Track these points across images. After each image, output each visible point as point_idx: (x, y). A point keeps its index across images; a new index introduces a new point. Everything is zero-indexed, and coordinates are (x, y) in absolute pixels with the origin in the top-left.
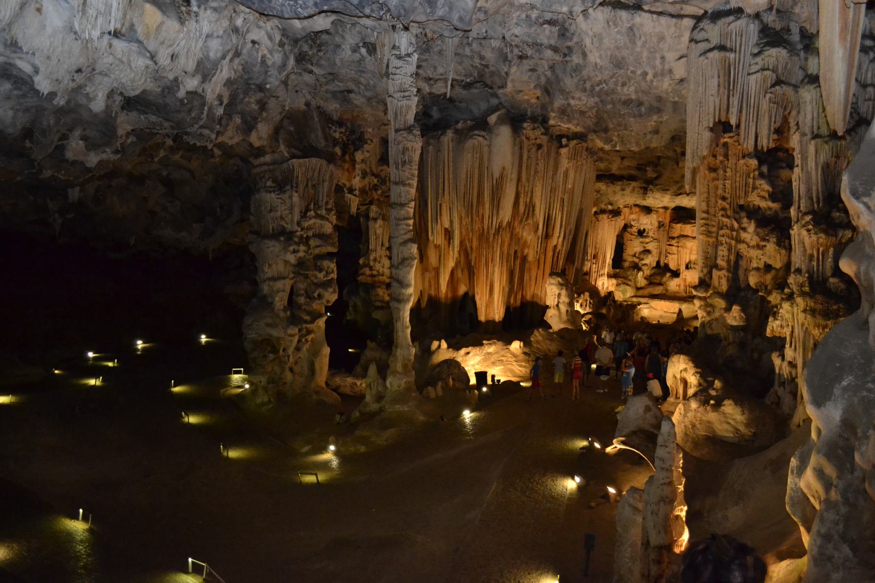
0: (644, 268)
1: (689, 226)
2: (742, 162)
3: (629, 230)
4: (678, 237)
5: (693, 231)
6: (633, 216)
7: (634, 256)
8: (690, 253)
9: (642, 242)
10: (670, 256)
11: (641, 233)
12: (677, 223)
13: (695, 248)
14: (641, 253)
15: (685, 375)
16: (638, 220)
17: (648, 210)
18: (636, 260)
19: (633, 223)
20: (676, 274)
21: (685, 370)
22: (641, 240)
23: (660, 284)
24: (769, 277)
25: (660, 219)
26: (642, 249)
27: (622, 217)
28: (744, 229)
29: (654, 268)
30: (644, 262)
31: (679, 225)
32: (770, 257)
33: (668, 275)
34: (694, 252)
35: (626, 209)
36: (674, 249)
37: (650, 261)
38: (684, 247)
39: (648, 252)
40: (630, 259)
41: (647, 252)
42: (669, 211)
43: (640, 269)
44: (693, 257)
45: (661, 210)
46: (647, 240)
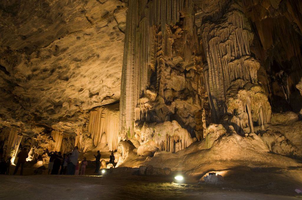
2: (170, 39)
15: (177, 133)
21: (177, 130)
24: (177, 94)
28: (165, 70)
32: (175, 86)
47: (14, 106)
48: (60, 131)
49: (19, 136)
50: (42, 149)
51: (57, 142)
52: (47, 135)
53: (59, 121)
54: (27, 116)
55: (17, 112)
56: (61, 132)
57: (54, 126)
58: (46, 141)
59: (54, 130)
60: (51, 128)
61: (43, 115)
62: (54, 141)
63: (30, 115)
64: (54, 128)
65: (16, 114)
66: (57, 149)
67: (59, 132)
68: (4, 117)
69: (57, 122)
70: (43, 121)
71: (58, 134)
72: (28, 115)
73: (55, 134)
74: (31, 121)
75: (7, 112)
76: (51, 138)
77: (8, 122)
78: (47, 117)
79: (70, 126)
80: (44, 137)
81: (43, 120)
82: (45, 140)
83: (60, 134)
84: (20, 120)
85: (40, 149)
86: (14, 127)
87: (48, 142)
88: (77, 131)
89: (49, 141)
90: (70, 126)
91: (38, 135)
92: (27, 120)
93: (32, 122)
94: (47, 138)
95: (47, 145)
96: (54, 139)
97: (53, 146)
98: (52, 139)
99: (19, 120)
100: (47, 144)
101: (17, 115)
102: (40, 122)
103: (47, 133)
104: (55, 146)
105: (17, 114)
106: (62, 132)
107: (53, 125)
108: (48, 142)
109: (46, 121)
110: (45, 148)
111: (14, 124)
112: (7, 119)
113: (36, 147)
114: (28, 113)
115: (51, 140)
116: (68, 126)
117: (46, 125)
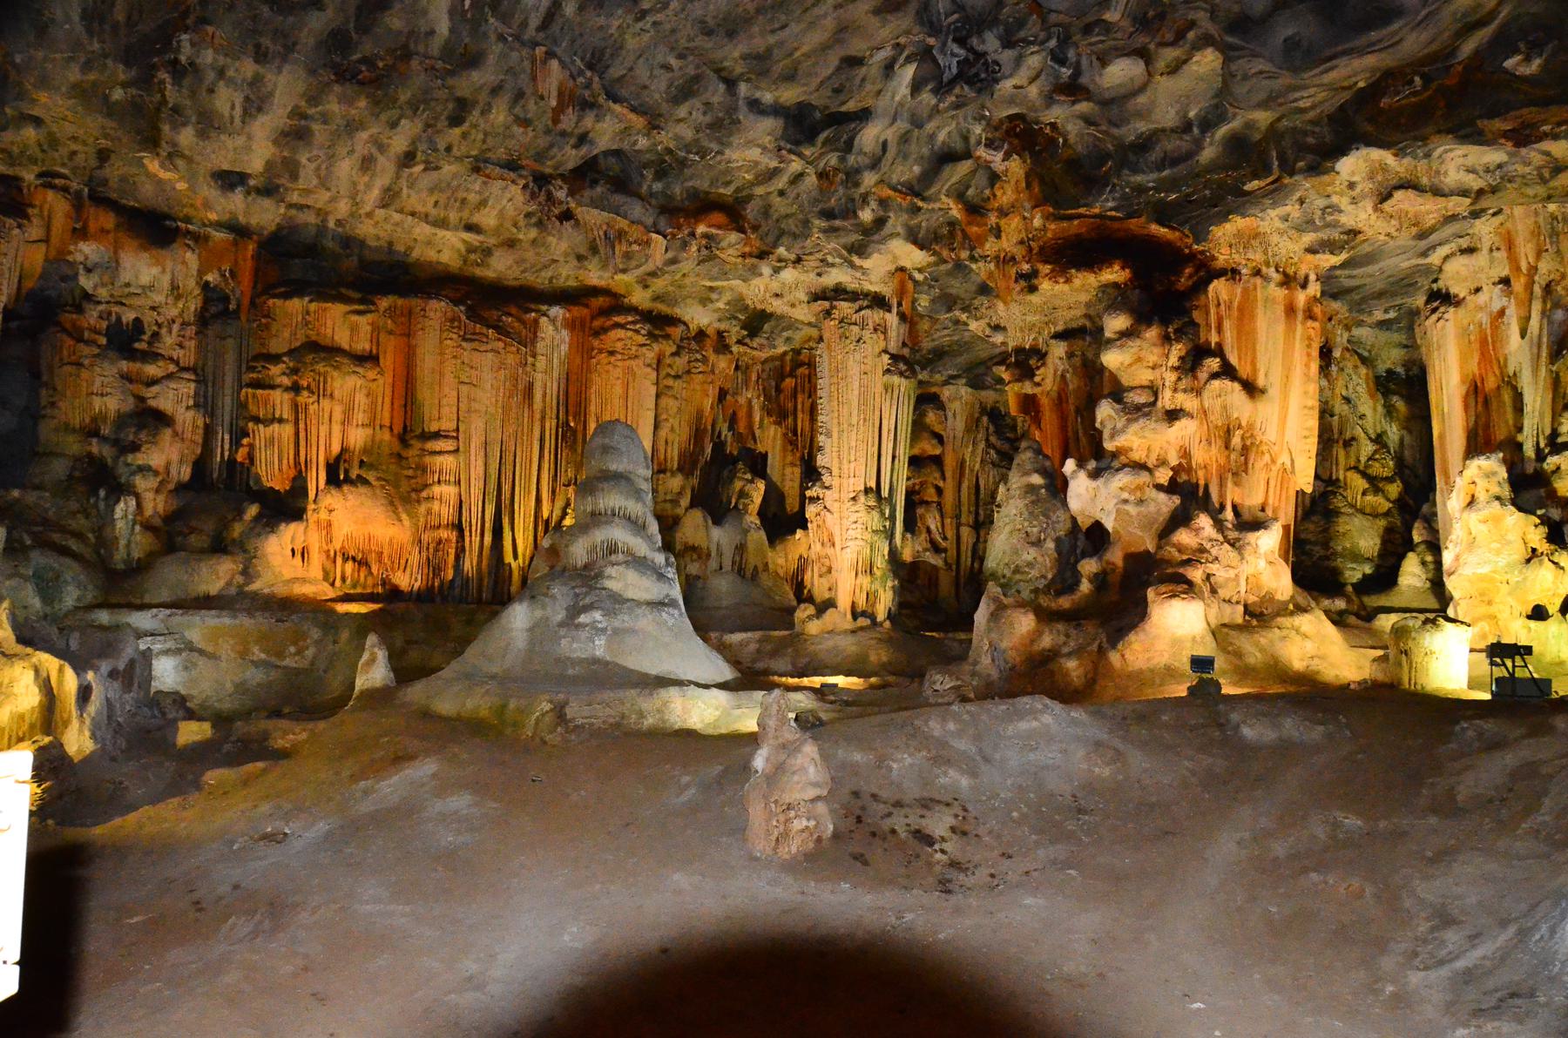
0: (143, 484)
1: (338, 309)
3: (68, 318)
4: (291, 352)
5: (354, 329)
6: (88, 250)
7: (91, 432)
8: (347, 421)
9: (127, 377)
10: (262, 432)
11: (127, 341)
12: (287, 296)
13: (361, 399)
14: (122, 420)
16: (113, 266)
17: (156, 228)
18: (95, 447)
19: (86, 282)
20: (286, 506)
22: (124, 365)
23: (220, 547)
25: (210, 278)
26: (129, 405)
27: (35, 232)
29: (181, 488)
30: (140, 459)
31: (296, 305)
33: (253, 510)
34: (360, 417)
35: (50, 195)
36: (280, 401)
37: (167, 456)
38: (320, 391)
39: (161, 419)
40: (73, 446)
41: (153, 420)
42: (251, 247)
43: (120, 489)
44: (358, 437)
45: (219, 236)
46: (152, 370)
47: (857, 46)
48: (1289, 281)
49: (896, 379)
50: (1144, 477)
51: (1273, 392)
52: (1166, 339)
53: (1342, 151)
54: (965, 167)
55: (869, 136)
56: (1304, 286)
57: (1236, 224)
58: (1167, 400)
59: (1233, 273)
60: (1192, 256)
61: (1141, 115)
62: (1251, 389)
63: (982, 152)
64: (1223, 258)
65: (858, 171)
66: (1284, 459)
67: (1282, 284)
68: (755, 228)
69: (1315, 170)
70: (1140, 190)
71: (1280, 310)
72: (967, 155)
73: (1245, 313)
74: (993, 219)
75: (774, 164)
76: (1213, 364)
77: (788, 275)
78: (1186, 127)
79: (1464, 193)
80: (1139, 359)
81: (1135, 171)
82: (1153, 389)
83: (1290, 310)
84: (896, 222)
85: (1123, 479)
86: (844, 304)
87: (1187, 402)
88: (1470, 251)
89: (1198, 392)
90: (1464, 193)
91: (1042, 356)
92: (956, 212)
93: (1012, 226)
94: (1174, 360)
95: (1185, 430)
96: (1244, 372)
97: (1236, 441)
98: (1228, 371)
99: (889, 227)
100: (1178, 425)
101: (869, 179)
102: (1097, 211)
103: (1165, 322)
104: (1270, 434)
105: (875, 164)
106: (1314, 289)
107: (1223, 217)
108: (1187, 402)
109: (1172, 184)
110: (1162, 462)
111: (838, 276)
112: (775, 246)
113: (1081, 464)
114: (966, 139)
115: (1215, 376)
116: (1437, 192)
117: (1156, 229)
